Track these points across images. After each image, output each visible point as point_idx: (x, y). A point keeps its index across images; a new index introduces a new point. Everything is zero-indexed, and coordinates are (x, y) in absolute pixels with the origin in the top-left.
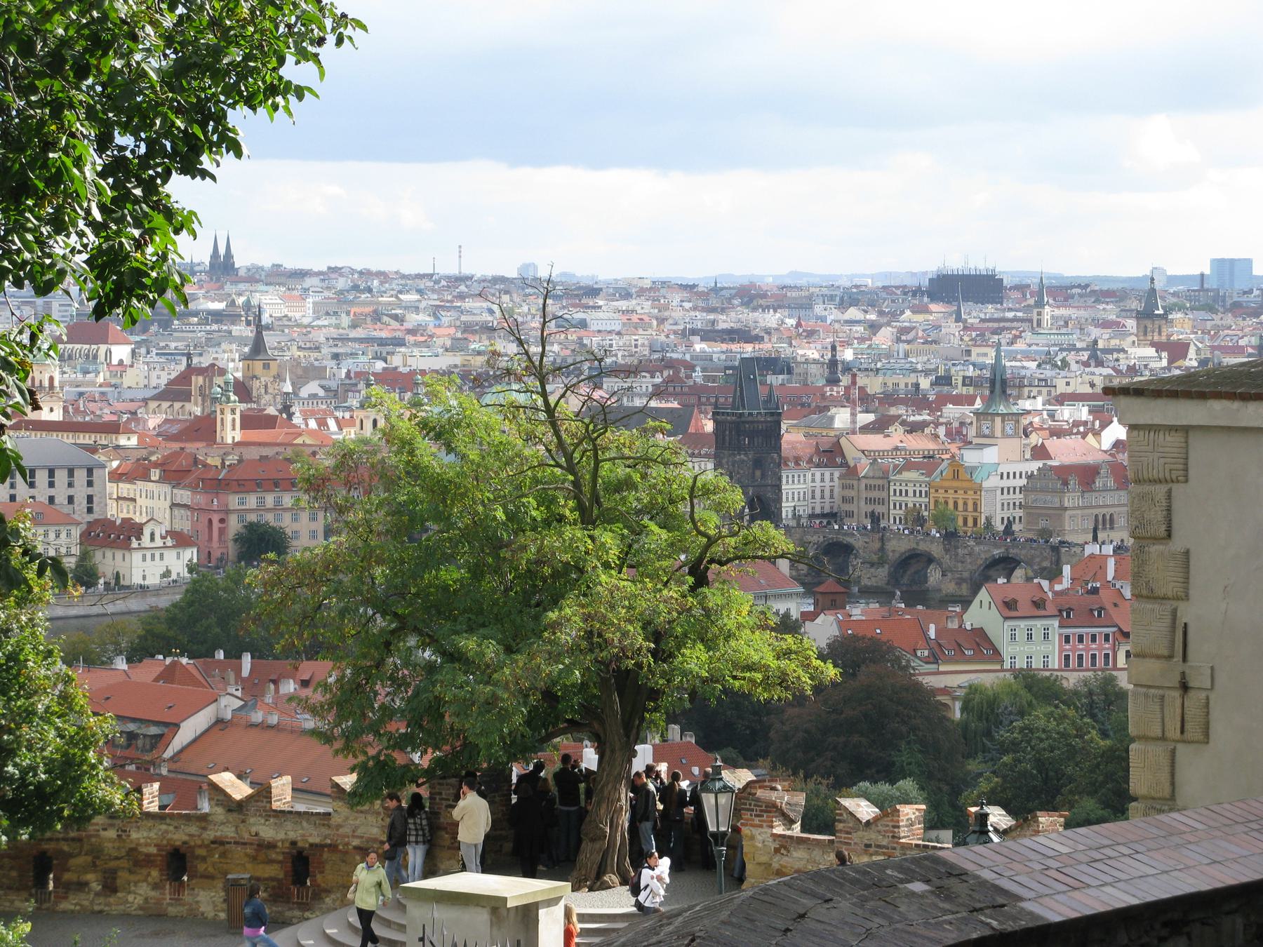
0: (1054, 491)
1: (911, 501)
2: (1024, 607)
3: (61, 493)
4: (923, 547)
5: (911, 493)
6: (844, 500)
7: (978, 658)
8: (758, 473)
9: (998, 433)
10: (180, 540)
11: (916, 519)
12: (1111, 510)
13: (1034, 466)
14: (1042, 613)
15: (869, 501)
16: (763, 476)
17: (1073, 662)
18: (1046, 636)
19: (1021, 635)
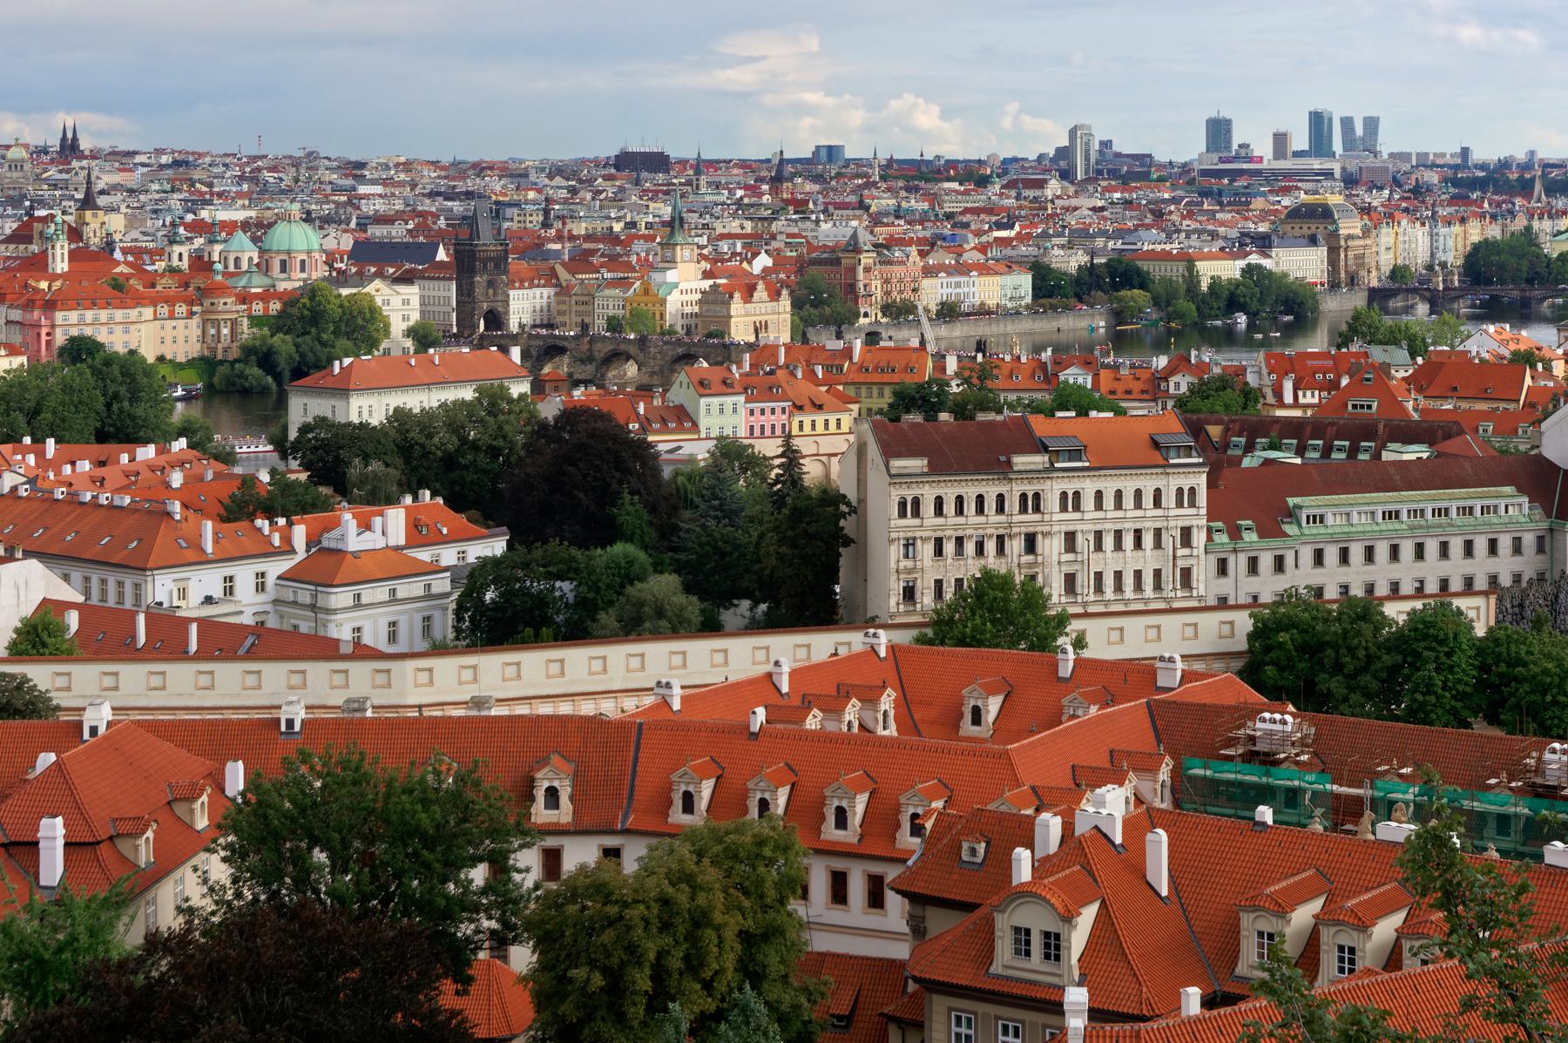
0: (723, 303)
1: (611, 312)
4: (623, 347)
5: (611, 307)
6: (560, 313)
7: (680, 429)
8: (491, 291)
9: (679, 260)
11: (614, 325)
12: (766, 318)
13: (706, 284)
14: (730, 390)
15: (578, 313)
16: (495, 294)
17: (757, 432)
18: (735, 410)
19: (715, 410)
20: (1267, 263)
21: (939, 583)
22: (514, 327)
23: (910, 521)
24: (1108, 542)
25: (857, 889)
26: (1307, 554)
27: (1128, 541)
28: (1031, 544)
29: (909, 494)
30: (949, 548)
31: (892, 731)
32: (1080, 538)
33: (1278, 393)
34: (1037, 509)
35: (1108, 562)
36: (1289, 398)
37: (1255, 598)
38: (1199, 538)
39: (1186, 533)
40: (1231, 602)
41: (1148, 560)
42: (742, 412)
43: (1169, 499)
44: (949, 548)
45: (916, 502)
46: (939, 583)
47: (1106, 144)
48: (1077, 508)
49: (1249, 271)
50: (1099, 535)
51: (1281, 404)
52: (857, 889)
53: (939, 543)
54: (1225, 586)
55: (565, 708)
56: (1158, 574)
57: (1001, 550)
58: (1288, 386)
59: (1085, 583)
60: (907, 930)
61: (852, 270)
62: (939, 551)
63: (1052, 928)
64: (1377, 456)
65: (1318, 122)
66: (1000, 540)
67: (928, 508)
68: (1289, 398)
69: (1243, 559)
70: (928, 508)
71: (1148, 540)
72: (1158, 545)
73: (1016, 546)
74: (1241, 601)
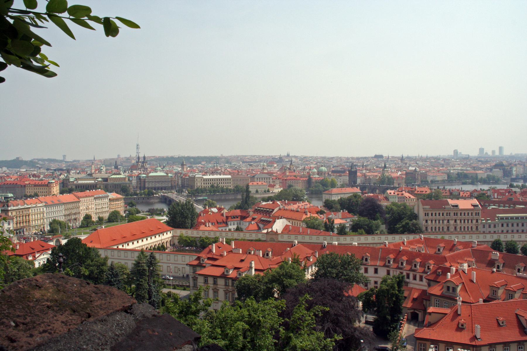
1: (374, 181)
2: (392, 194)
3: (266, 181)
10: (280, 187)
11: (374, 184)
20: (491, 174)
21: (432, 228)
22: (358, 183)
23: (427, 217)
24: (463, 221)
25: (418, 278)
26: (500, 225)
27: (466, 221)
28: (448, 221)
29: (427, 212)
30: (434, 222)
31: (424, 252)
32: (457, 220)
33: (494, 195)
34: (449, 215)
36: (496, 197)
37: (490, 232)
40: (485, 232)
42: (397, 198)
43: (474, 214)
44: (434, 222)
45: (428, 214)
46: (432, 228)
47: (460, 153)
48: (457, 215)
49: (488, 175)
51: (494, 198)
52: (418, 278)
53: (432, 221)
54: (484, 230)
55: (368, 245)
56: (472, 227)
57: (443, 222)
58: (496, 194)
60: (427, 285)
61: (415, 175)
63: (454, 287)
64: (514, 207)
65: (501, 149)
66: (443, 220)
67: (430, 215)
68: (496, 197)
69: (488, 226)
70: (430, 215)
71: (470, 221)
72: (472, 222)
73: (445, 222)
74: (488, 232)
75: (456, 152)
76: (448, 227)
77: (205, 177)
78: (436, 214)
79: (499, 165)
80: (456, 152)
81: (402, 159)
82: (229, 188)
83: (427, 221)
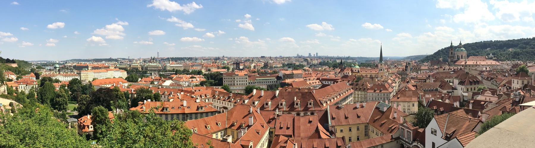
24: (240, 81)
27: (242, 81)
30: (228, 82)
35: (240, 83)
38: (247, 81)
39: (246, 81)
41: (243, 83)
43: (245, 78)
44: (228, 82)
50: (239, 81)
59: (238, 84)
62: (227, 81)
65: (317, 53)
67: (226, 79)
71: (243, 81)
73: (233, 82)
75: (298, 55)
76: (234, 84)
77: (171, 66)
78: (229, 78)
79: (306, 60)
80: (298, 55)
81: (270, 58)
82: (182, 70)
83: (225, 82)
